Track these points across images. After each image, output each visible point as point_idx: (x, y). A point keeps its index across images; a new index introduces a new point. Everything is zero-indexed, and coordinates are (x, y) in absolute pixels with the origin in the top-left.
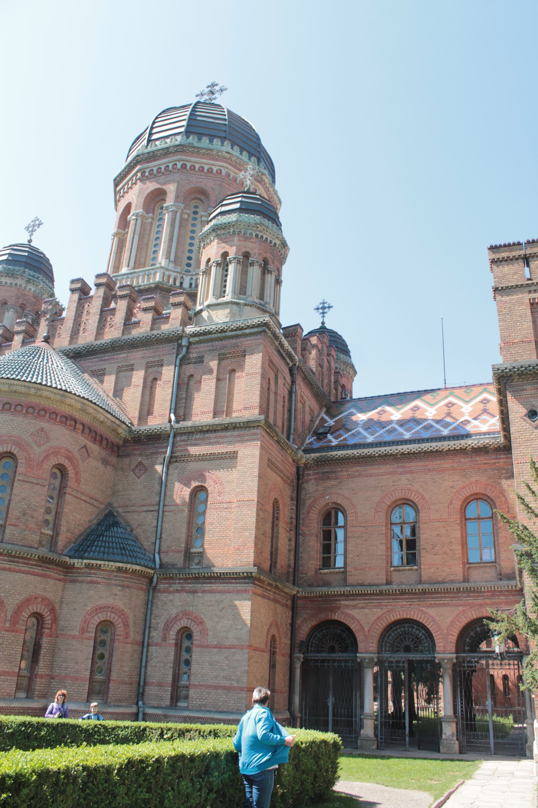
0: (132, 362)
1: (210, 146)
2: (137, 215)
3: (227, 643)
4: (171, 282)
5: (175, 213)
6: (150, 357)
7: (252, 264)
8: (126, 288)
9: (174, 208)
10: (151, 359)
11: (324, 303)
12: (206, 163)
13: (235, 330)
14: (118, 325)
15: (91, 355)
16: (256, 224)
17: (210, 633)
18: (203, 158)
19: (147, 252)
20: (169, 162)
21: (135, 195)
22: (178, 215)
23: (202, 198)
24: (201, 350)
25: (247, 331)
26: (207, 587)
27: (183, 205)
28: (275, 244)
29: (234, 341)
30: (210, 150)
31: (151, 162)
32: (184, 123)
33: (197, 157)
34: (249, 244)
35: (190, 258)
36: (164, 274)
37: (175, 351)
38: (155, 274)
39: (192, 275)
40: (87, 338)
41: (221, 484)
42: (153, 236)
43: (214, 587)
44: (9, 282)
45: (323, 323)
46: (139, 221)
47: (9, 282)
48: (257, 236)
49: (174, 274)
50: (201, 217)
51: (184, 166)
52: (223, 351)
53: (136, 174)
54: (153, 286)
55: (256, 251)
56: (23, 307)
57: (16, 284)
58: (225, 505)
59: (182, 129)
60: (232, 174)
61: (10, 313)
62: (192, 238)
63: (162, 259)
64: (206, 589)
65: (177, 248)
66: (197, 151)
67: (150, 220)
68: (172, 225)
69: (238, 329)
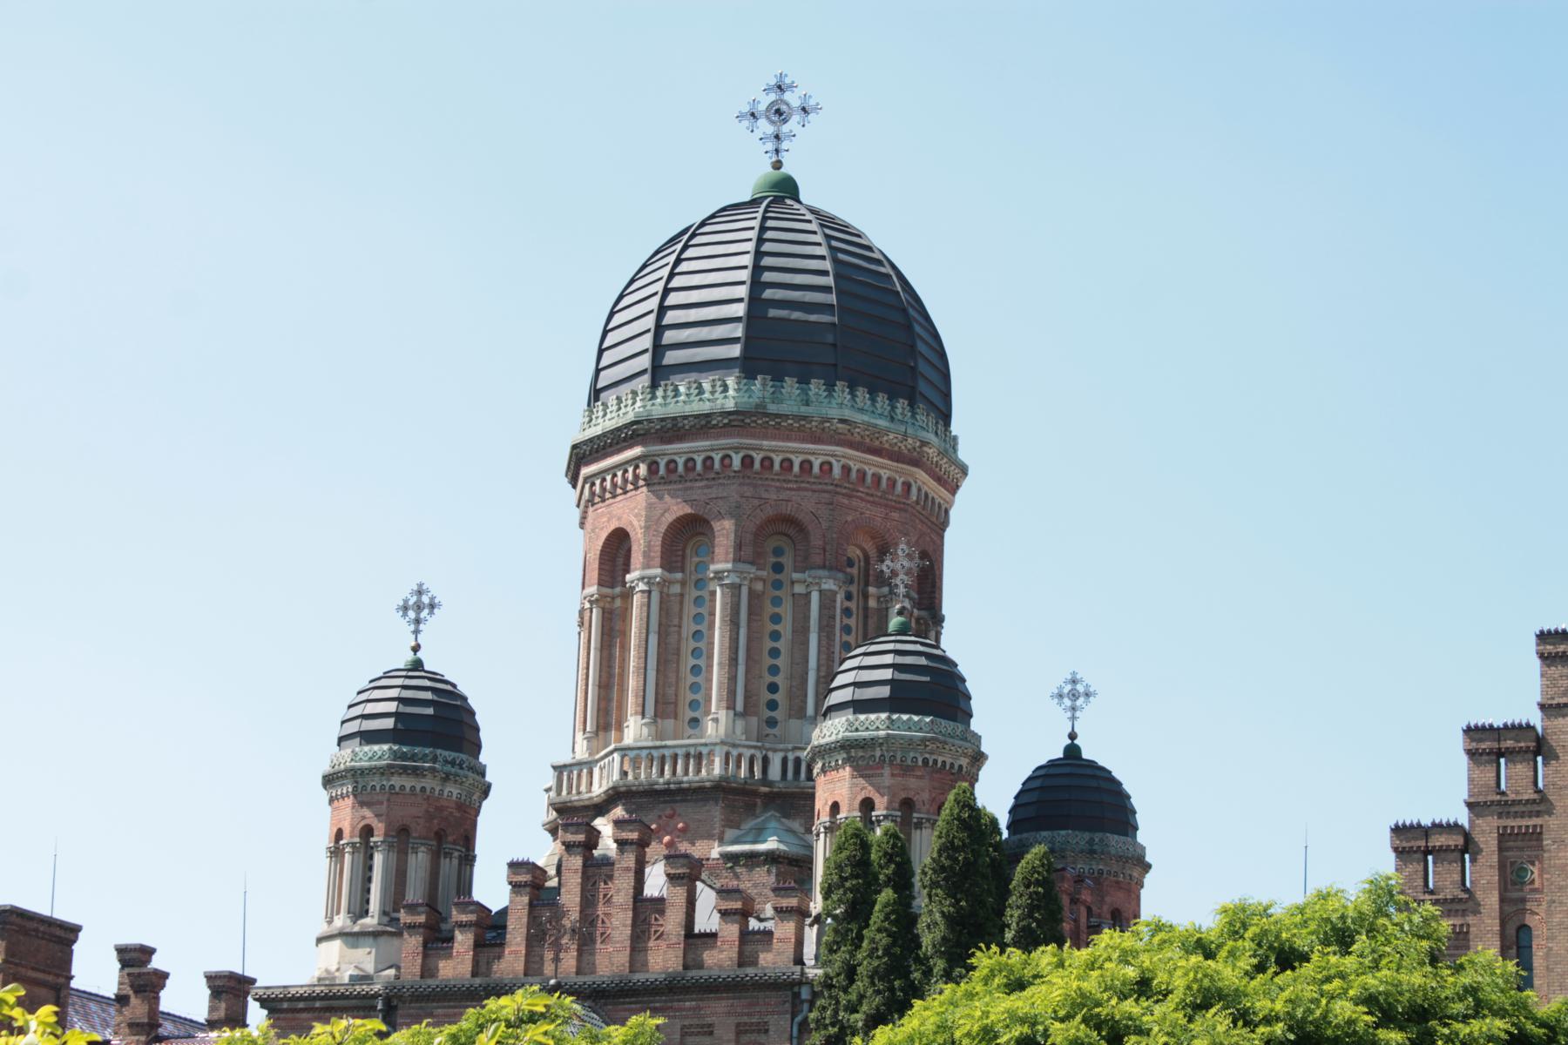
0: (709, 1020)
1: (804, 410)
2: (649, 581)
4: (743, 773)
5: (735, 588)
6: (743, 1014)
7: (919, 825)
8: (682, 861)
10: (745, 1019)
11: (1074, 682)
12: (798, 450)
14: (674, 940)
15: (627, 996)
16: (924, 740)
18: (789, 439)
19: (678, 671)
21: (633, 511)
22: (745, 591)
23: (792, 532)
27: (753, 569)
28: (961, 767)
30: (805, 418)
31: (670, 442)
32: (739, 310)
33: (774, 438)
34: (912, 782)
35: (773, 688)
36: (727, 755)
37: (788, 1006)
38: (711, 753)
39: (787, 750)
40: (611, 960)
42: (689, 627)
44: (408, 786)
45: (1072, 736)
46: (655, 596)
47: (408, 786)
48: (925, 761)
49: (748, 753)
50: (793, 583)
51: (747, 462)
53: (635, 462)
54: (708, 784)
55: (926, 796)
56: (440, 836)
57: (423, 789)
59: (735, 351)
60: (855, 467)
61: (420, 855)
62: (775, 636)
63: (718, 708)
65: (747, 672)
66: (775, 424)
67: (676, 589)
68: (733, 622)
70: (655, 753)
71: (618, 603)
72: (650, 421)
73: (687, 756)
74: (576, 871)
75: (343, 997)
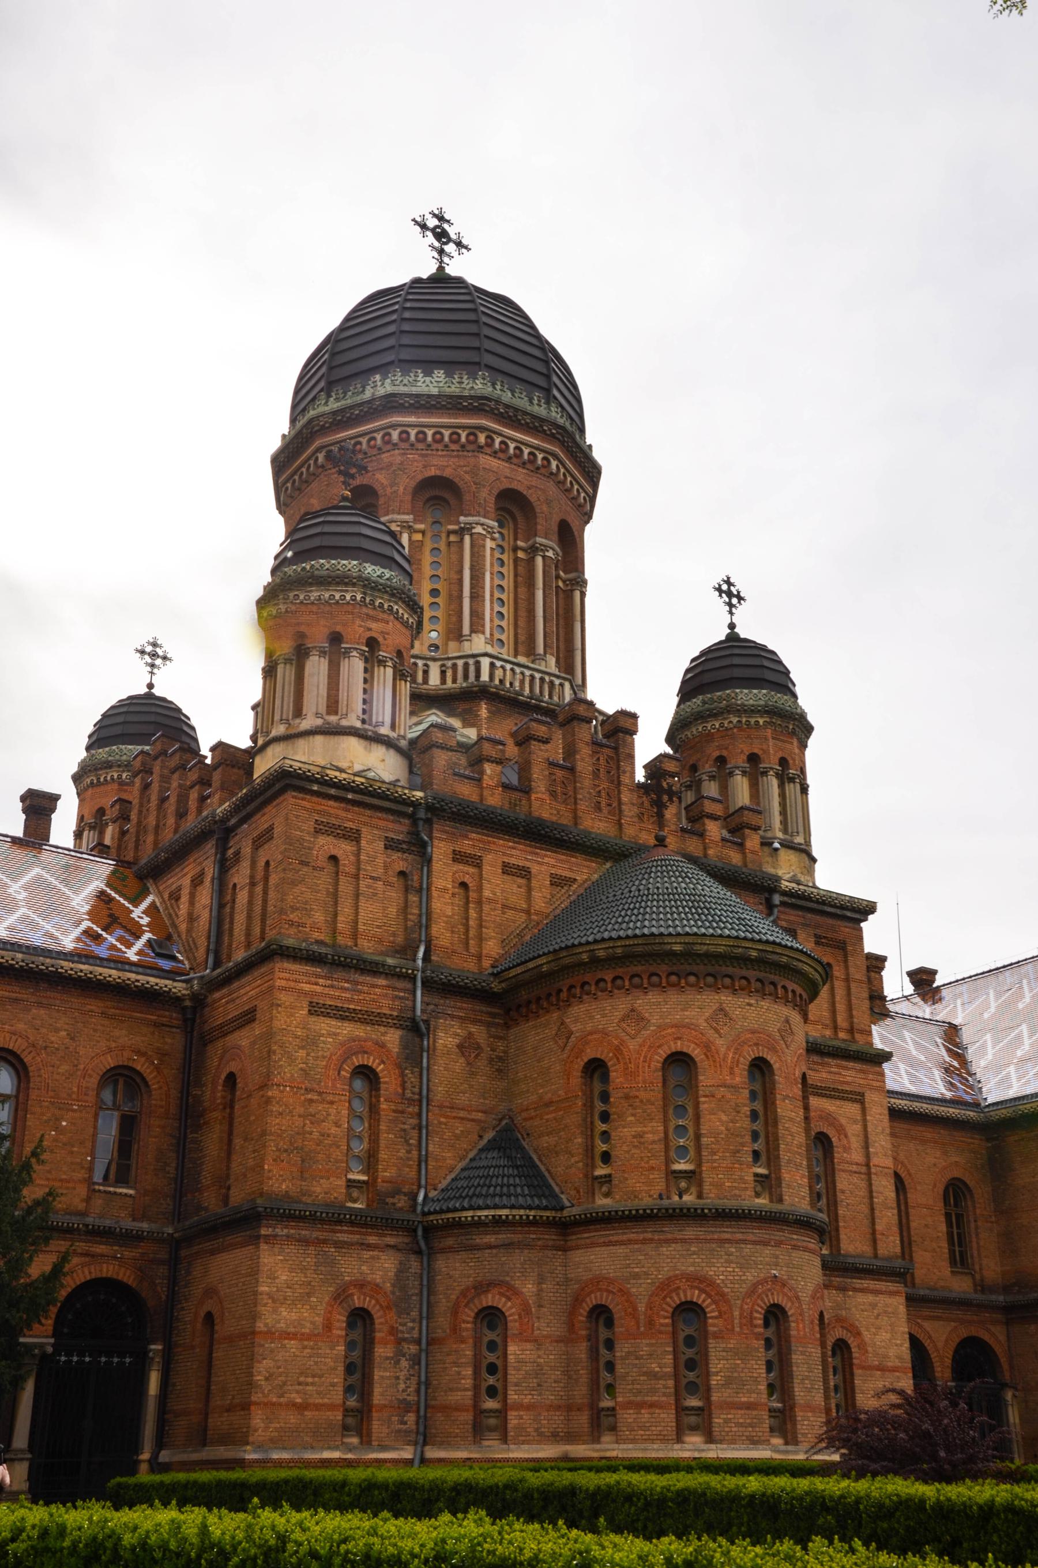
3: (890, 1364)
9: (550, 554)
13: (837, 907)
17: (870, 1349)
20: (537, 449)
24: (792, 918)
25: (849, 914)
26: (858, 1283)
29: (830, 921)
31: (505, 426)
41: (846, 1136)
43: (866, 1283)
47: (406, 616)
52: (818, 932)
58: (854, 1168)
64: (857, 1286)
69: (842, 907)
70: (518, 670)
71: (418, 537)
72: (498, 402)
73: (542, 680)
74: (587, 744)
75: (383, 796)
